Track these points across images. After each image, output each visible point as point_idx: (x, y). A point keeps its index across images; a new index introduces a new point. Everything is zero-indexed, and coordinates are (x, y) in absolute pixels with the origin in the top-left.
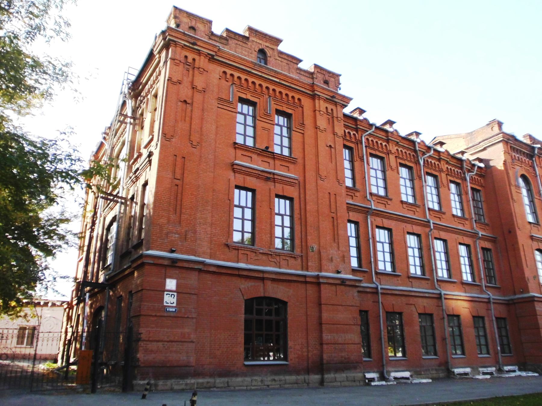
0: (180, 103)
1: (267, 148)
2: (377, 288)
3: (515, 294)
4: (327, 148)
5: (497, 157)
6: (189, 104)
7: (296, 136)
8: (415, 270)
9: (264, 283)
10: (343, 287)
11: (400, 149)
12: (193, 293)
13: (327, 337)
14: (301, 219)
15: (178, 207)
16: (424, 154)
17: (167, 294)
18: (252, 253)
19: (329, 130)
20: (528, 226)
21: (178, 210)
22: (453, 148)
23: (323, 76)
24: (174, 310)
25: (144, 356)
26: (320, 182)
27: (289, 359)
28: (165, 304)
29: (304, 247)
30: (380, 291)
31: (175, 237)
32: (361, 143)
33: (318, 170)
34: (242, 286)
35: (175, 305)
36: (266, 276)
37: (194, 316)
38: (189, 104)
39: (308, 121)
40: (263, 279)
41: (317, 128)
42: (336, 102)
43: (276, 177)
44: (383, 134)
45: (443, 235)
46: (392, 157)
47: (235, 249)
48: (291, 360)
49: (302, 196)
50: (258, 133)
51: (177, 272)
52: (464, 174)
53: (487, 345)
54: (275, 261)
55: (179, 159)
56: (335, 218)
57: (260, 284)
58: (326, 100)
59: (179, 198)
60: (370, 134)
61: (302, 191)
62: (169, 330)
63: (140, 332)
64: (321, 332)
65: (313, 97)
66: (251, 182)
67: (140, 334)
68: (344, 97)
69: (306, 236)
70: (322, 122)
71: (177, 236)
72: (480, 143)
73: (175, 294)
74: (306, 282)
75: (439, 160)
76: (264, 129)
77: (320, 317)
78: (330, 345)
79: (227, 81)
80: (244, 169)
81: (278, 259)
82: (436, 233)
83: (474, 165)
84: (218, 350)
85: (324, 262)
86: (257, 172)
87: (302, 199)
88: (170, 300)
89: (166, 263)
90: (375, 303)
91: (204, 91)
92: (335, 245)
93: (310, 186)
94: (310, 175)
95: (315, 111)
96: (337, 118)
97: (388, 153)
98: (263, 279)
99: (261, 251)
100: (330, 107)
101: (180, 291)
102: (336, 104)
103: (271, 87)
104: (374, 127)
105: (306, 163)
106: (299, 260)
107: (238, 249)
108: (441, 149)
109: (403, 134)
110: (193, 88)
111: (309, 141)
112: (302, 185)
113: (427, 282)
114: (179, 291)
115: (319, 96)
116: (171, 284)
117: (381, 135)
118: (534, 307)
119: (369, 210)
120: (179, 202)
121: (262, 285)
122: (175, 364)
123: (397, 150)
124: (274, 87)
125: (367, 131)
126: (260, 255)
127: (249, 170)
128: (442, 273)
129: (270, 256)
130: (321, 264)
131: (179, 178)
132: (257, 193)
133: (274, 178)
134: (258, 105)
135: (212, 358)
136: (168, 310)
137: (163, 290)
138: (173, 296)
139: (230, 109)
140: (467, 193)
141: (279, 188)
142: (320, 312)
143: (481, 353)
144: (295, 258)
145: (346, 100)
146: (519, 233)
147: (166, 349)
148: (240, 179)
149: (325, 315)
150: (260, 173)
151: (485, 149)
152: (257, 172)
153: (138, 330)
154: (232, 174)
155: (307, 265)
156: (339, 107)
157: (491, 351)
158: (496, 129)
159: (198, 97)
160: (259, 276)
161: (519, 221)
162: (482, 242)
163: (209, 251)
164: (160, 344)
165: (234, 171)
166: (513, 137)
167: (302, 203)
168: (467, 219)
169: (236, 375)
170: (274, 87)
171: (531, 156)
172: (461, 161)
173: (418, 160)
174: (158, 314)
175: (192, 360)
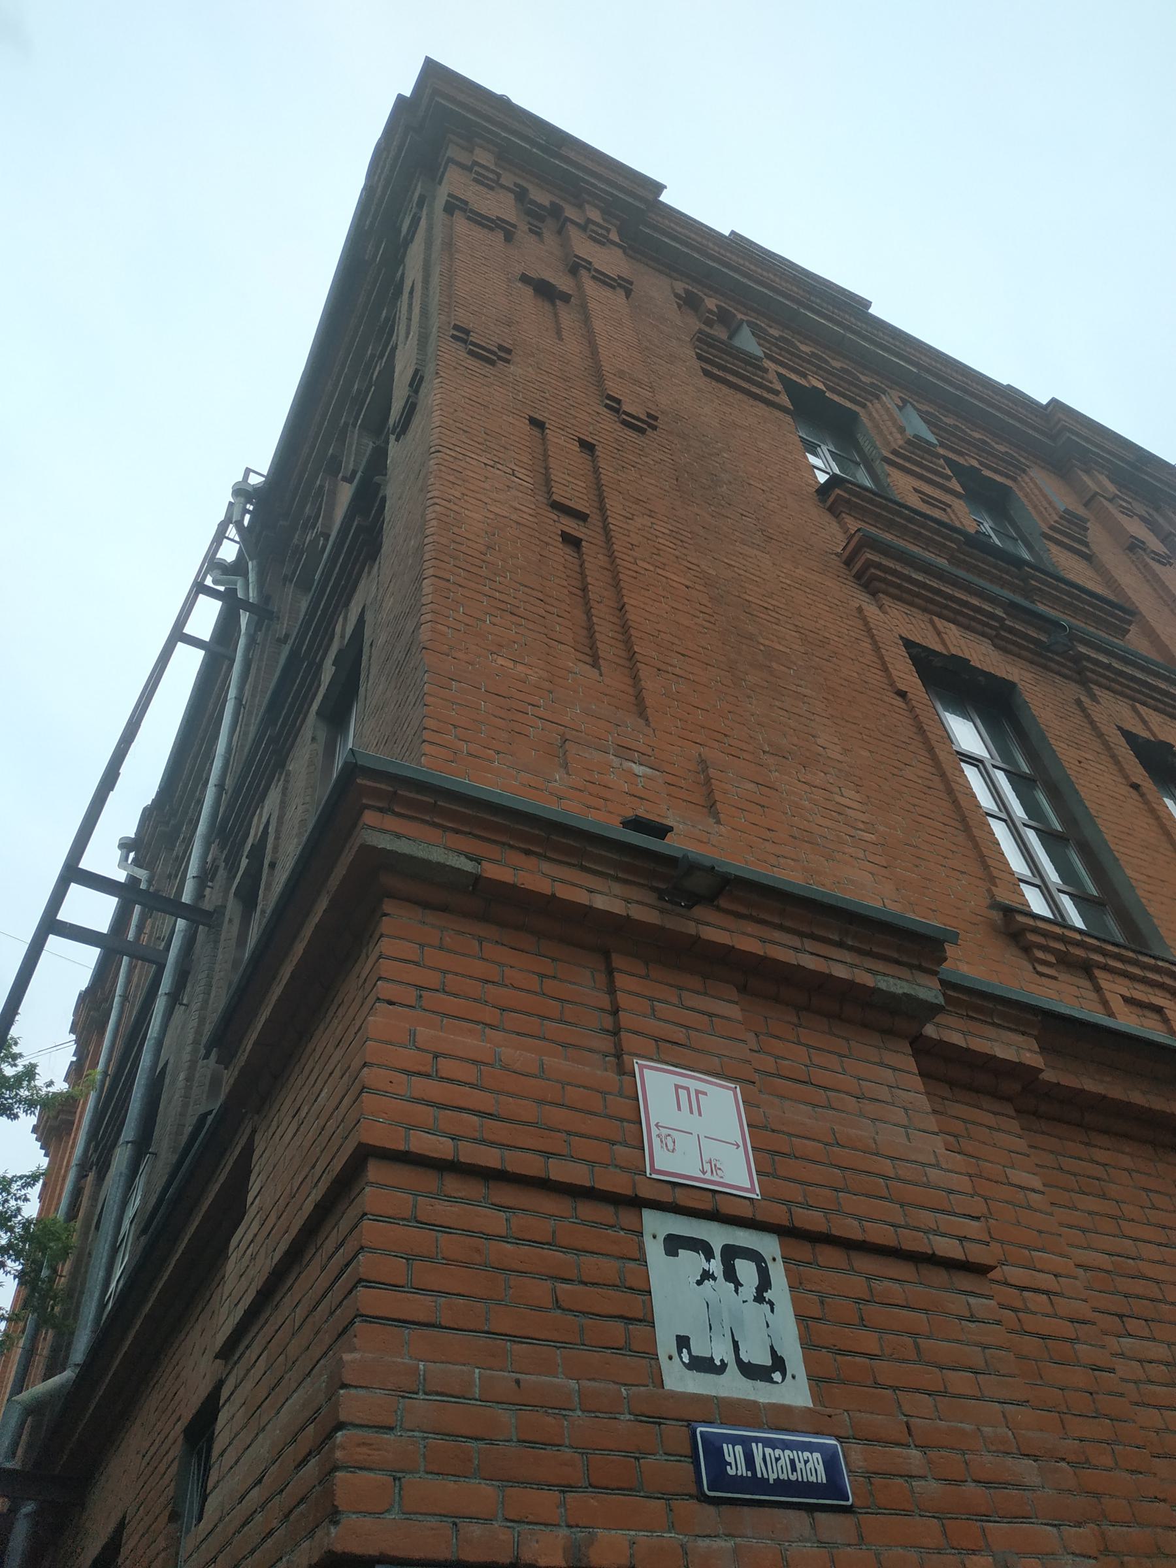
15: (605, 631)
17: (673, 1244)
21: (608, 648)
24: (813, 1468)
28: (679, 1380)
35: (794, 1392)
73: (768, 1245)
101: (812, 1220)
116: (695, 1126)
136: (734, 1455)
138: (746, 1270)
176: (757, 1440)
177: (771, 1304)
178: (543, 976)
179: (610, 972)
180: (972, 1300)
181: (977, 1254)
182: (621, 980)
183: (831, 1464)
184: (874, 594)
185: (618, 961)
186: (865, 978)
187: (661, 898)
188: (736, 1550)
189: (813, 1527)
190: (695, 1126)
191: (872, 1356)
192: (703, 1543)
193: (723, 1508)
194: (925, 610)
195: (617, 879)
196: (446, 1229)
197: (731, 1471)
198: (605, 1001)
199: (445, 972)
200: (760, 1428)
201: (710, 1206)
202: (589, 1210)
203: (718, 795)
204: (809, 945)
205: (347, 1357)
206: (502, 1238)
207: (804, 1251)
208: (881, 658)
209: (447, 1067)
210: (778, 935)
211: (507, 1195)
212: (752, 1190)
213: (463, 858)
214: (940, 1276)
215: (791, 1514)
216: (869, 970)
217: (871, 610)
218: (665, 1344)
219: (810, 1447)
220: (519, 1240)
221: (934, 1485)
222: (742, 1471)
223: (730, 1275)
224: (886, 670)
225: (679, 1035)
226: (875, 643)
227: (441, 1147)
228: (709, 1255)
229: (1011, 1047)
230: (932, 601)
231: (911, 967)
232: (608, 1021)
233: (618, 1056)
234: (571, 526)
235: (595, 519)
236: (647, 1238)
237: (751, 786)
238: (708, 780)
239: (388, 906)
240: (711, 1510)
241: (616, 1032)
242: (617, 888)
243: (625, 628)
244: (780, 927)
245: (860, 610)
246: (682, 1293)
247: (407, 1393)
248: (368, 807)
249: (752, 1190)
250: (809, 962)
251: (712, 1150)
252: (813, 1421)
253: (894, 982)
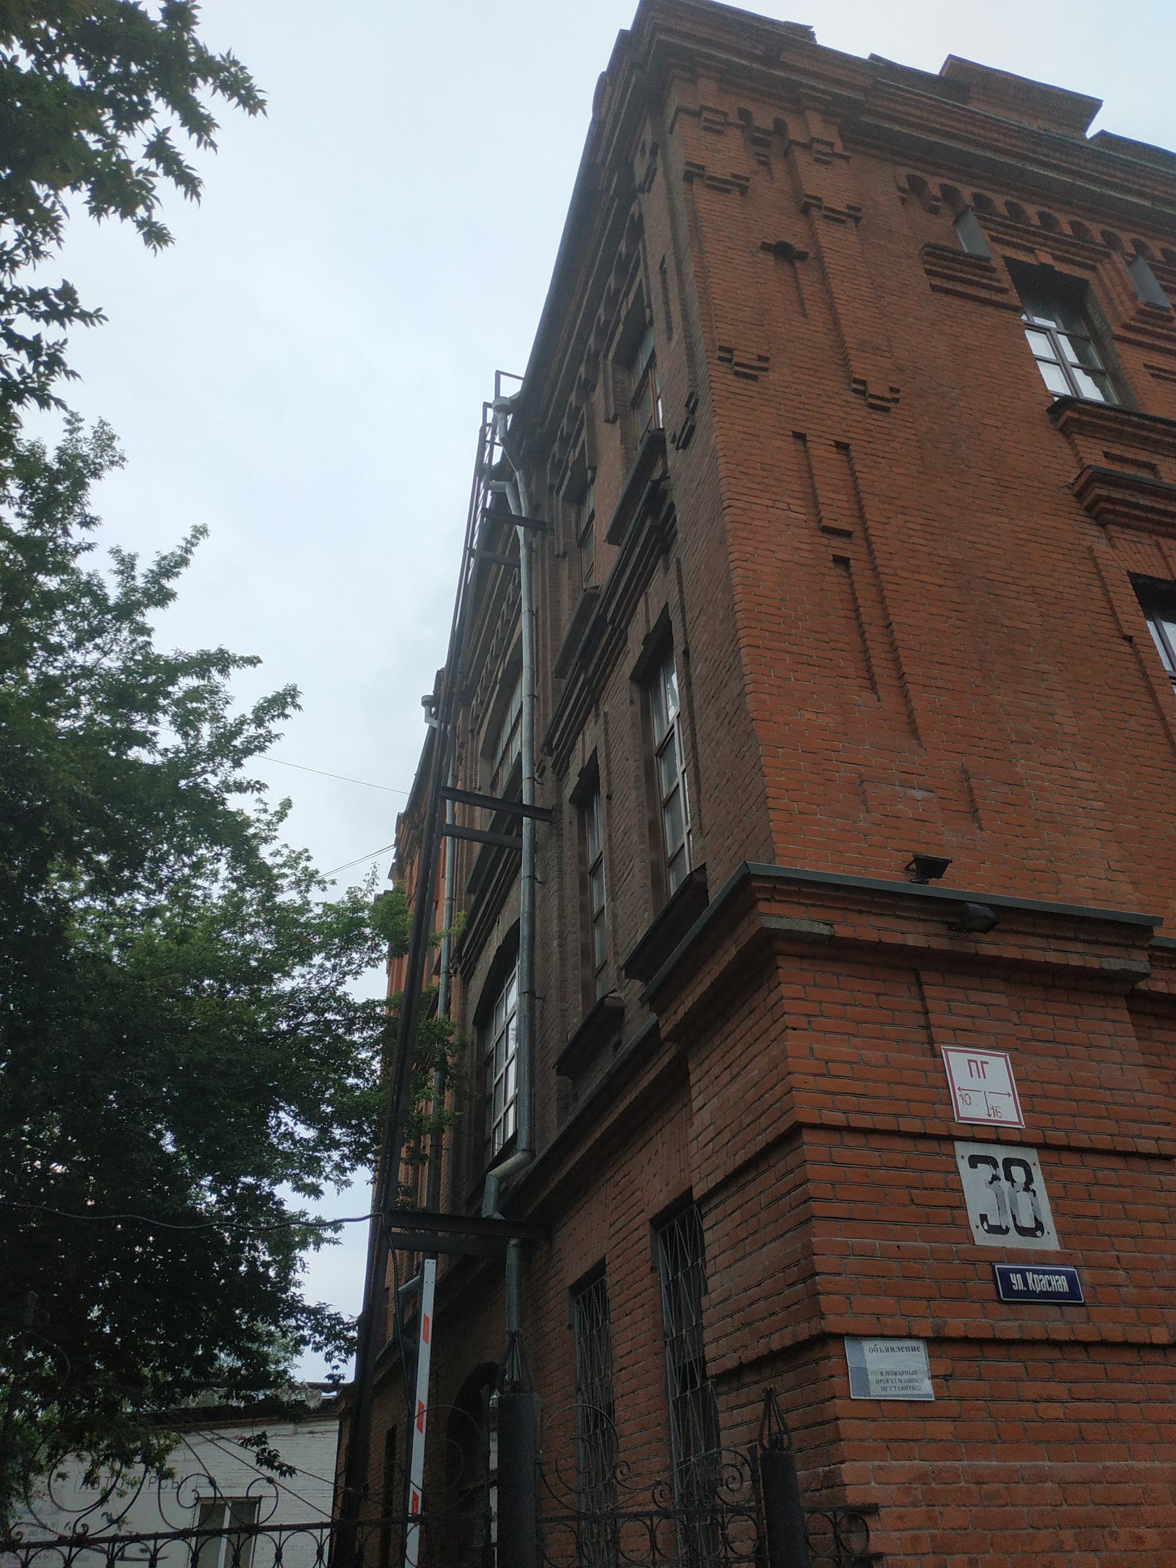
15: (878, 653)
17: (974, 1161)
21: (883, 674)
24: (1061, 1284)
28: (982, 1238)
35: (1050, 1241)
55: (821, 451)
59: (869, 611)
62: (1073, 1468)
63: (854, 1496)
67: (862, 1514)
73: (1031, 1156)
101: (1058, 1138)
114: (1047, 1142)
116: (983, 1085)
131: (843, 524)
136: (1016, 1279)
137: (939, 1129)
138: (1018, 1173)
153: (832, 1482)
154: (1094, 530)
176: (1029, 1270)
177: (1034, 1192)
178: (878, 995)
179: (920, 985)
180: (1161, 1177)
182: (928, 990)
183: (1071, 1280)
184: (1103, 525)
185: (925, 976)
186: (1093, 963)
187: (950, 929)
188: (1020, 1327)
189: (1062, 1314)
190: (983, 1085)
191: (1096, 1218)
192: (1002, 1324)
193: (1013, 1306)
194: (1151, 532)
195: (920, 920)
196: (848, 1165)
197: (1015, 1288)
198: (917, 1005)
199: (820, 1002)
200: (1030, 1264)
201: (995, 1135)
202: (924, 1146)
203: (979, 802)
204: (1054, 944)
205: (813, 1239)
206: (879, 1167)
207: (1052, 1156)
208: (1110, 601)
209: (834, 1068)
210: (1031, 941)
211: (876, 1141)
212: (1020, 1123)
213: (822, 926)
214: (1142, 1164)
215: (1048, 1307)
216: (1097, 956)
217: (1101, 546)
218: (974, 1220)
219: (1059, 1273)
220: (889, 1168)
221: (1134, 1291)
222: (1021, 1287)
223: (1009, 1177)
224: (1114, 614)
225: (968, 1023)
226: (1104, 586)
227: (838, 1118)
228: (995, 1164)
230: (1159, 523)
231: (1126, 946)
232: (922, 1020)
233: (931, 1042)
234: (839, 546)
236: (958, 1158)
237: (1005, 788)
238: (970, 790)
239: (781, 961)
240: (1005, 1307)
241: (928, 1027)
242: (920, 927)
244: (1033, 934)
245: (1090, 549)
246: (978, 1190)
247: (844, 1256)
248: (759, 899)
249: (1020, 1123)
250: (1053, 958)
251: (993, 1100)
252: (1059, 1258)
253: (1113, 962)
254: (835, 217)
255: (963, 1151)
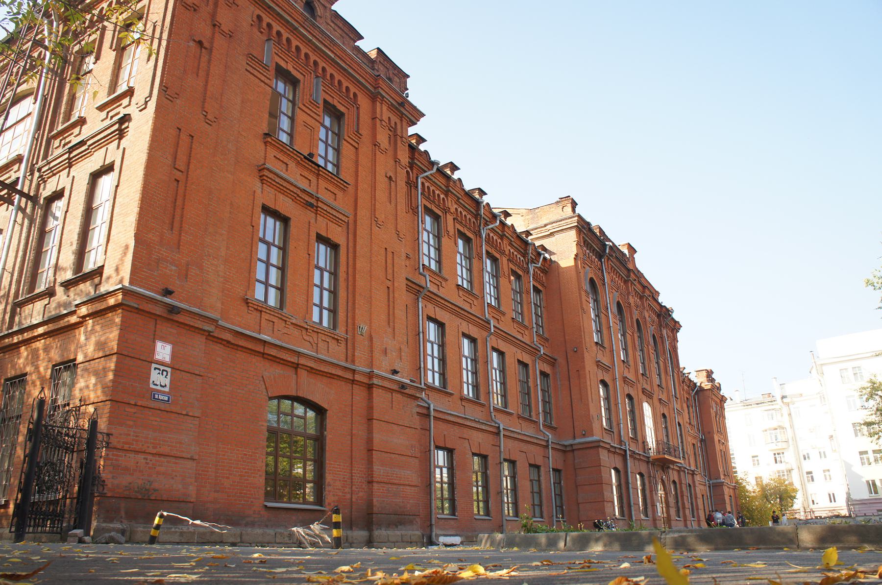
0: (192, 44)
1: (311, 155)
2: (429, 408)
3: (574, 438)
4: (386, 179)
5: (564, 251)
6: (206, 48)
7: (347, 150)
8: (468, 391)
9: (296, 373)
10: (399, 395)
11: (459, 209)
12: (197, 372)
13: (379, 470)
14: (347, 280)
15: (177, 218)
16: (486, 224)
17: (155, 369)
18: (280, 321)
19: (390, 153)
20: (595, 348)
21: (176, 225)
22: (519, 224)
23: (385, 70)
24: (166, 398)
25: (113, 477)
26: (375, 229)
27: (327, 502)
29: (350, 326)
30: (432, 413)
31: (171, 270)
32: (417, 187)
33: (373, 210)
34: (266, 374)
35: (167, 389)
36: (303, 361)
37: (196, 415)
38: (206, 48)
39: (365, 131)
40: (296, 366)
41: (375, 145)
42: (403, 114)
43: (320, 204)
44: (443, 181)
45: (503, 346)
46: (450, 218)
47: (256, 309)
48: (329, 504)
49: (351, 244)
50: (299, 128)
51: (174, 331)
52: (527, 264)
53: (541, 506)
54: (311, 340)
55: (184, 136)
56: (391, 290)
57: (290, 372)
58: (391, 107)
60: (427, 176)
61: (351, 236)
64: (370, 462)
65: (374, 97)
66: (285, 205)
68: (415, 108)
69: (354, 309)
70: (383, 138)
71: (174, 268)
72: (545, 226)
73: (169, 370)
74: (353, 382)
75: (502, 237)
76: (306, 125)
77: (370, 440)
78: (382, 485)
79: (261, 32)
80: (278, 180)
81: (315, 339)
82: (493, 341)
83: (539, 254)
84: (228, 478)
85: (377, 354)
86: (295, 190)
87: (351, 250)
88: (159, 379)
89: (158, 310)
90: (423, 432)
91: (231, 36)
92: (390, 330)
93: (362, 231)
94: (363, 214)
95: (374, 119)
96: (402, 137)
97: (446, 211)
98: (296, 366)
99: (294, 321)
100: (394, 119)
101: (177, 366)
102: (402, 116)
103: (322, 64)
104: (435, 167)
105: (359, 195)
106: (343, 345)
107: (261, 311)
108: (509, 221)
109: (468, 187)
110: (214, 25)
111: (365, 161)
112: (351, 228)
113: (481, 409)
115: (383, 97)
116: (163, 351)
117: (441, 181)
118: (598, 454)
119: (421, 290)
120: (178, 212)
121: (295, 376)
122: (165, 497)
123: (456, 209)
124: (324, 65)
125: (425, 172)
126: (291, 327)
127: (285, 184)
128: (497, 401)
129: (304, 331)
130: (372, 356)
131: (182, 168)
132: (292, 223)
133: (317, 207)
134: (301, 84)
135: (218, 491)
136: (156, 396)
138: (165, 373)
139: (263, 78)
140: (528, 292)
141: (322, 226)
142: (370, 431)
143: (534, 516)
144: (338, 340)
145: (415, 115)
146: (586, 355)
147: (150, 468)
148: (268, 196)
149: (377, 437)
150: (299, 192)
151: (552, 234)
152: (295, 190)
155: (354, 355)
156: (404, 123)
157: (545, 515)
158: (569, 209)
159: (220, 42)
160: (292, 360)
161: (587, 339)
162: (541, 362)
163: (219, 305)
164: (141, 457)
165: (262, 179)
166: (589, 224)
167: (351, 255)
168: (526, 327)
169: (252, 524)
170: (324, 65)
171: (600, 257)
172: (526, 243)
173: (480, 231)
174: (140, 403)
175: (192, 490)
181: (201, 374)
201: (162, 364)
218: (151, 382)
229: (228, 336)
235: (185, 174)
243: (182, 216)
252: (168, 393)
254: (223, 33)
255: (154, 366)
